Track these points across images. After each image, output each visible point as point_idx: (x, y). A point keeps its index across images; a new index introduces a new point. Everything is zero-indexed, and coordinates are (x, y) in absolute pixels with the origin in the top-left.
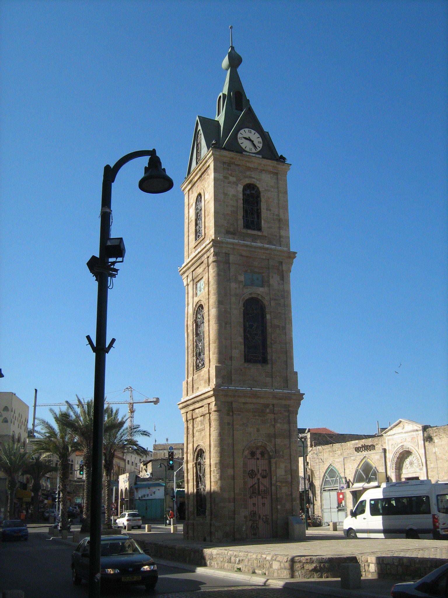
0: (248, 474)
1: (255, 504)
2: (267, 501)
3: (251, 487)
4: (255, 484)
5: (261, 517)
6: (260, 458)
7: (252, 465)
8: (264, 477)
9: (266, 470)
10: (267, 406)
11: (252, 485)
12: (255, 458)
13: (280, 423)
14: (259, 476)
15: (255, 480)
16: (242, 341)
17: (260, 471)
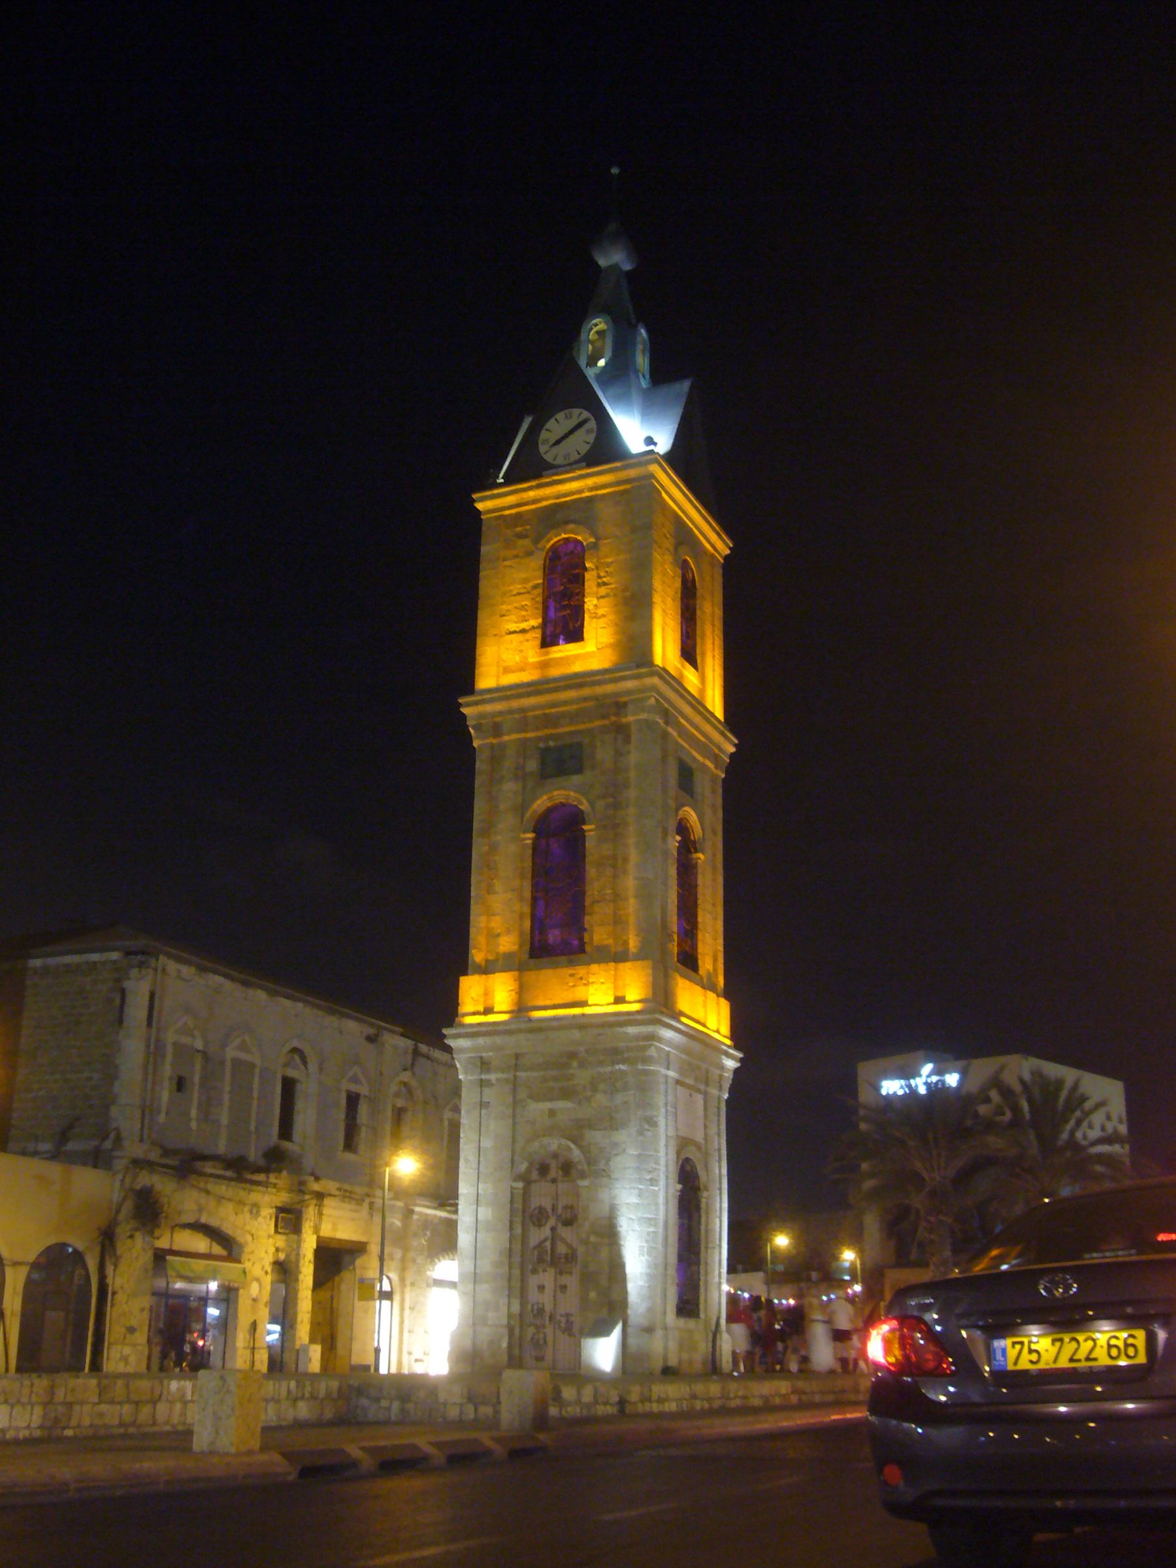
0: (531, 1216)
1: (543, 1287)
2: (572, 1282)
3: (535, 1248)
4: (545, 1240)
5: (558, 1317)
6: (560, 1178)
7: (542, 1195)
8: (568, 1223)
9: (572, 1207)
10: (572, 1055)
11: (537, 1242)
12: (549, 1177)
13: (605, 1093)
14: (552, 1222)
15: (546, 1232)
16: (527, 910)
17: (560, 1211)
